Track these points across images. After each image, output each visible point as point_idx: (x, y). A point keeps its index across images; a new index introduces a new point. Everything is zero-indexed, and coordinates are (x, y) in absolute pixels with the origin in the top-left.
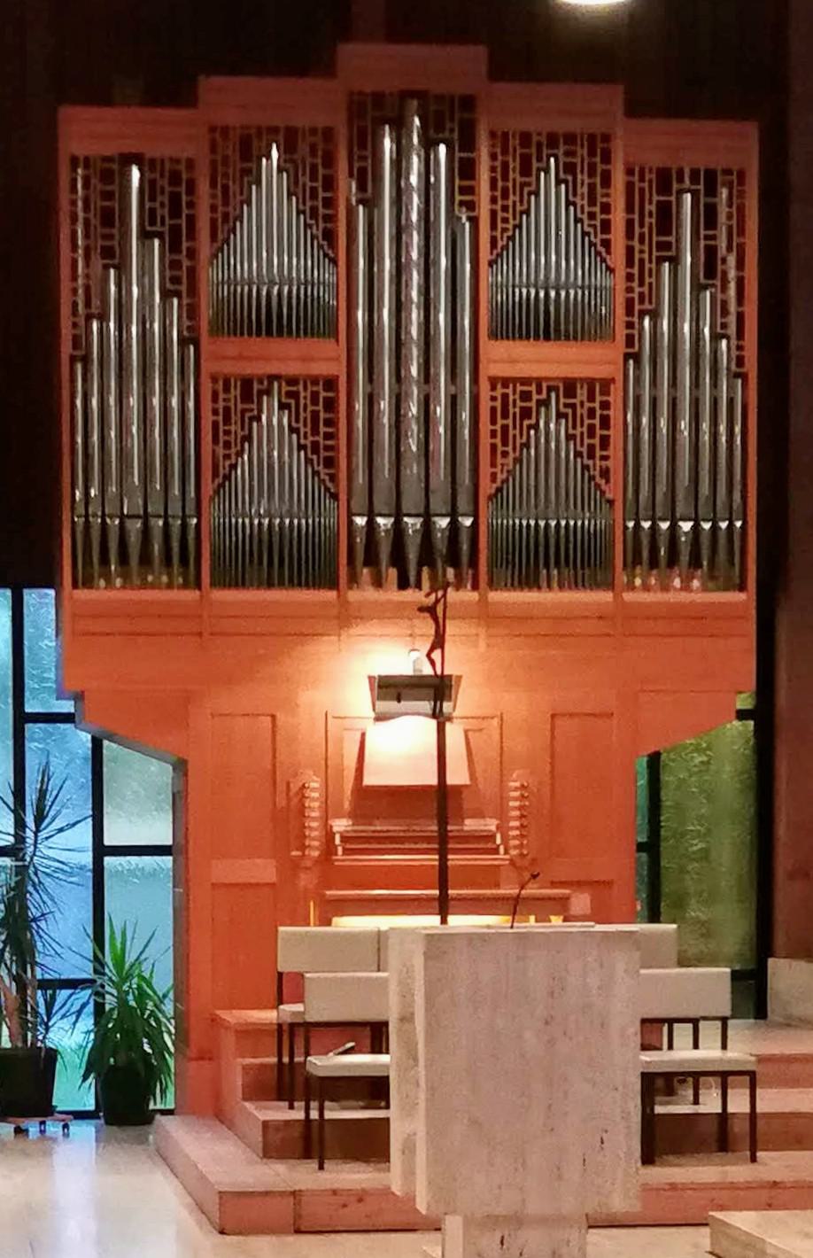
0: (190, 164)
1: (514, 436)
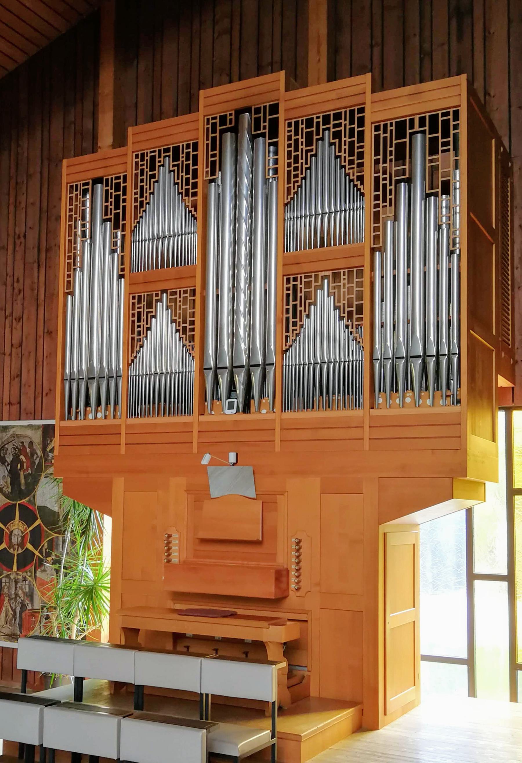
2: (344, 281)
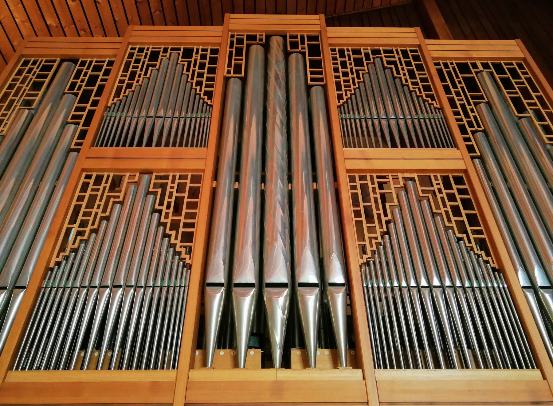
1: (379, 215)
2: (439, 186)
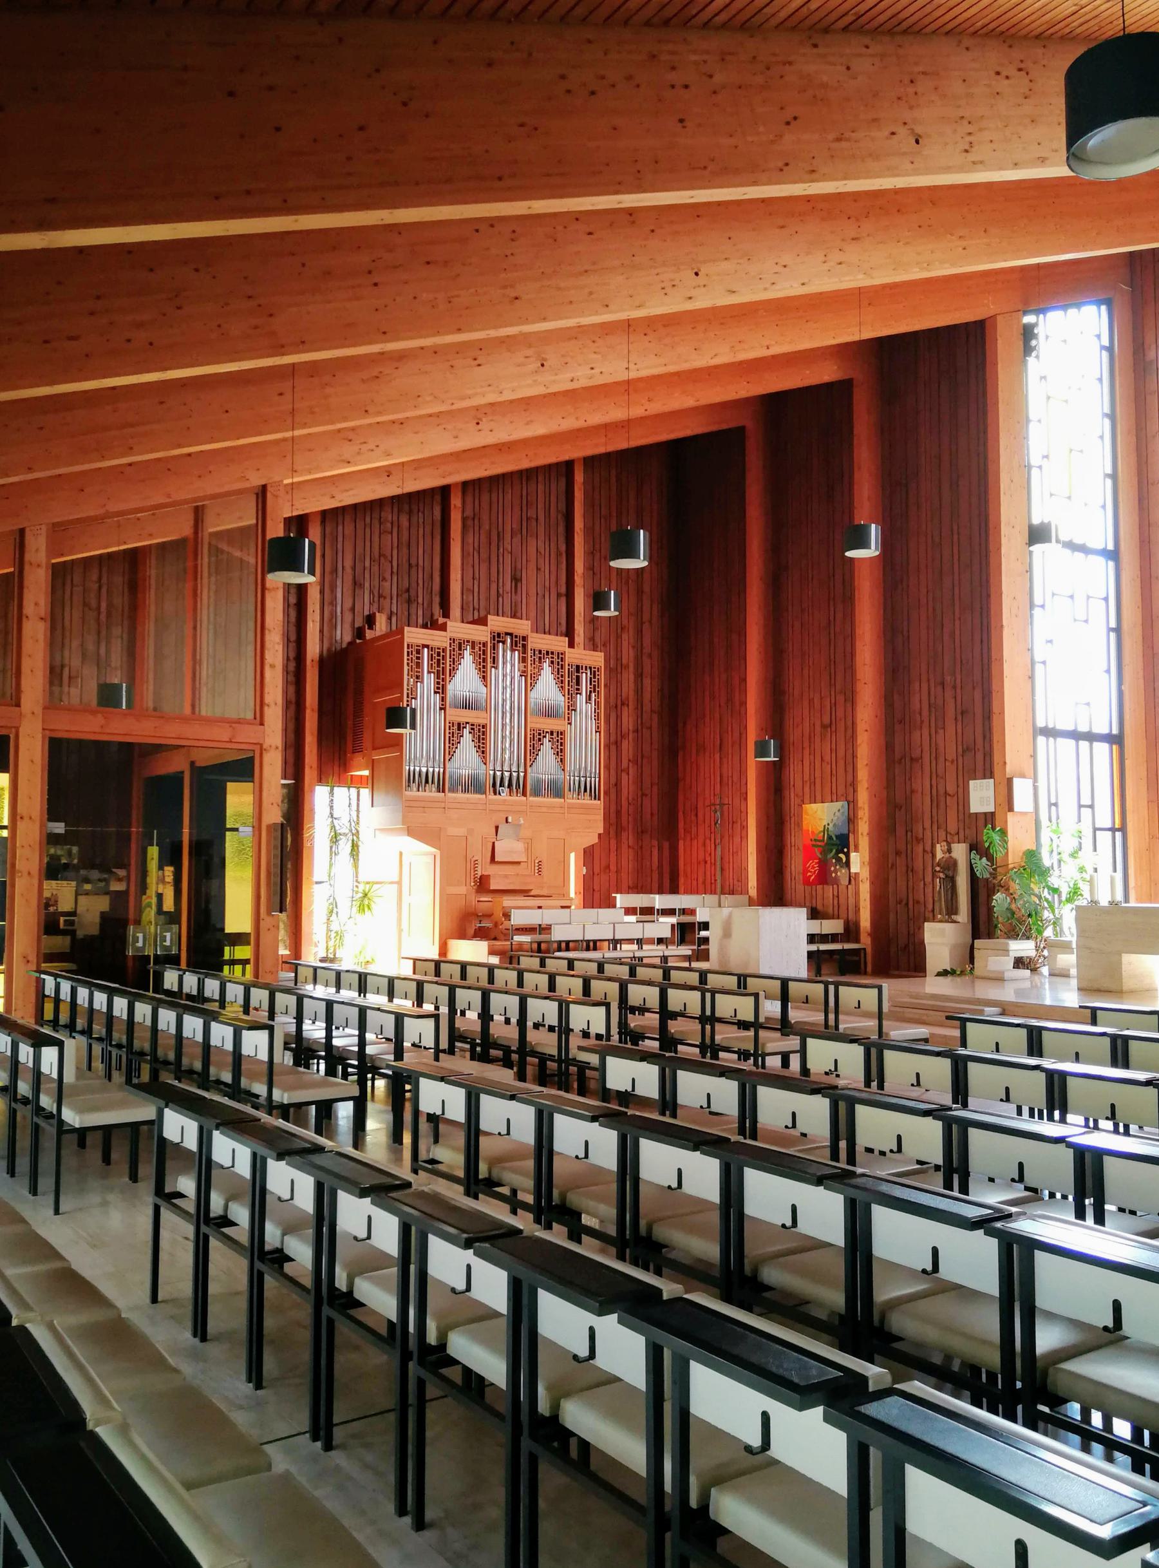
0: (444, 650)
